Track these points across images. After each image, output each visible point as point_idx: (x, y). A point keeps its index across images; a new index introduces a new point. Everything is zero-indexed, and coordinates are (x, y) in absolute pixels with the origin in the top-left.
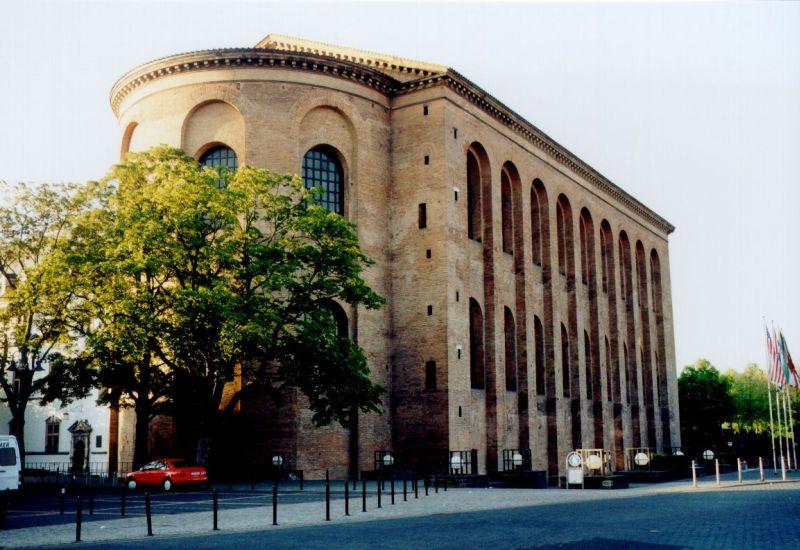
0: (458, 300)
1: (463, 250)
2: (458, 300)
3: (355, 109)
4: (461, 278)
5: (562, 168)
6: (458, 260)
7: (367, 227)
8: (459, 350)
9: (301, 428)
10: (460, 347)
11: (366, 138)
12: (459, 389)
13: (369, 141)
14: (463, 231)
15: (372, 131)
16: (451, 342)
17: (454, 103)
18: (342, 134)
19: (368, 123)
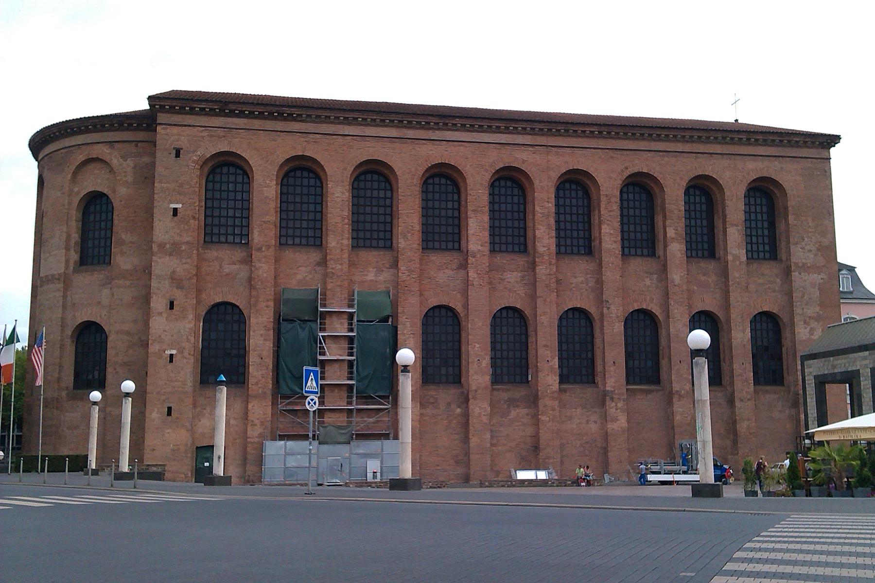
0: (172, 306)
1: (189, 260)
2: (172, 306)
3: (115, 153)
4: (180, 287)
5: (432, 135)
6: (174, 272)
7: (123, 254)
8: (171, 356)
9: (65, 429)
10: (174, 352)
11: (126, 176)
12: (169, 390)
13: (130, 178)
14: (187, 243)
15: (134, 168)
16: (153, 348)
17: (175, 125)
18: (107, 179)
19: (130, 162)
